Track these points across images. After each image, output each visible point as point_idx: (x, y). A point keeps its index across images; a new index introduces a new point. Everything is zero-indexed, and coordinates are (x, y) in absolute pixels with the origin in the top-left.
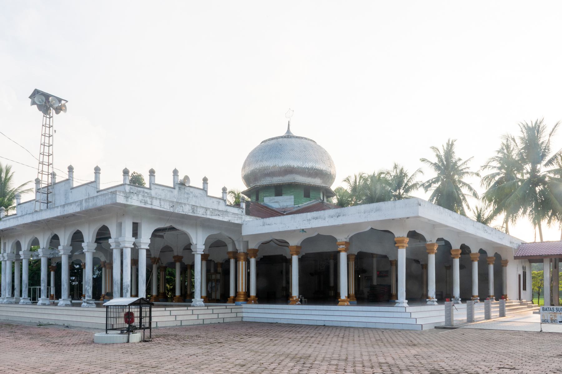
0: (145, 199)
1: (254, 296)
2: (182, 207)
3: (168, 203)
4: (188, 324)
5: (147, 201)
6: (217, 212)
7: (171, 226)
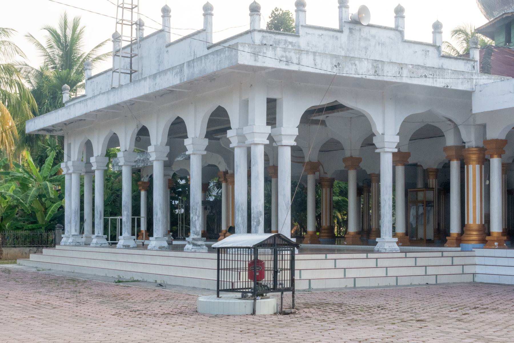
0: (287, 54)
1: (498, 233)
2: (356, 65)
3: (329, 60)
4: (368, 285)
5: (291, 58)
6: (421, 72)
7: (336, 101)
